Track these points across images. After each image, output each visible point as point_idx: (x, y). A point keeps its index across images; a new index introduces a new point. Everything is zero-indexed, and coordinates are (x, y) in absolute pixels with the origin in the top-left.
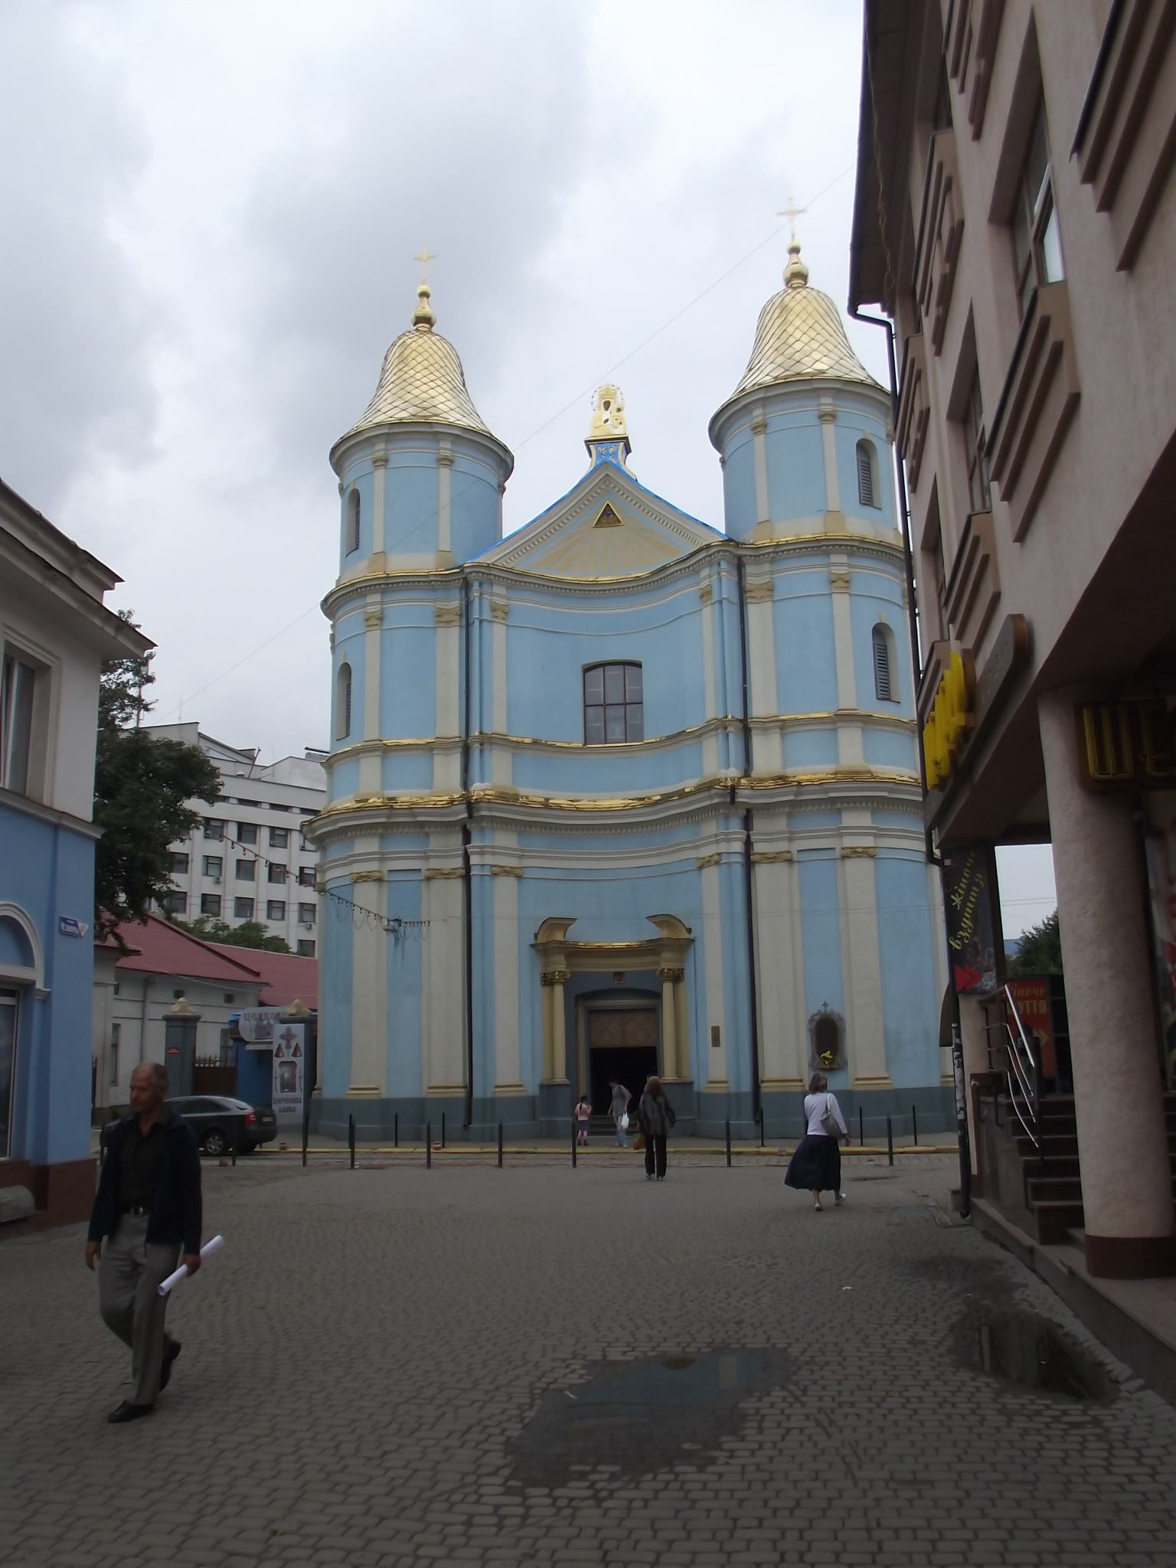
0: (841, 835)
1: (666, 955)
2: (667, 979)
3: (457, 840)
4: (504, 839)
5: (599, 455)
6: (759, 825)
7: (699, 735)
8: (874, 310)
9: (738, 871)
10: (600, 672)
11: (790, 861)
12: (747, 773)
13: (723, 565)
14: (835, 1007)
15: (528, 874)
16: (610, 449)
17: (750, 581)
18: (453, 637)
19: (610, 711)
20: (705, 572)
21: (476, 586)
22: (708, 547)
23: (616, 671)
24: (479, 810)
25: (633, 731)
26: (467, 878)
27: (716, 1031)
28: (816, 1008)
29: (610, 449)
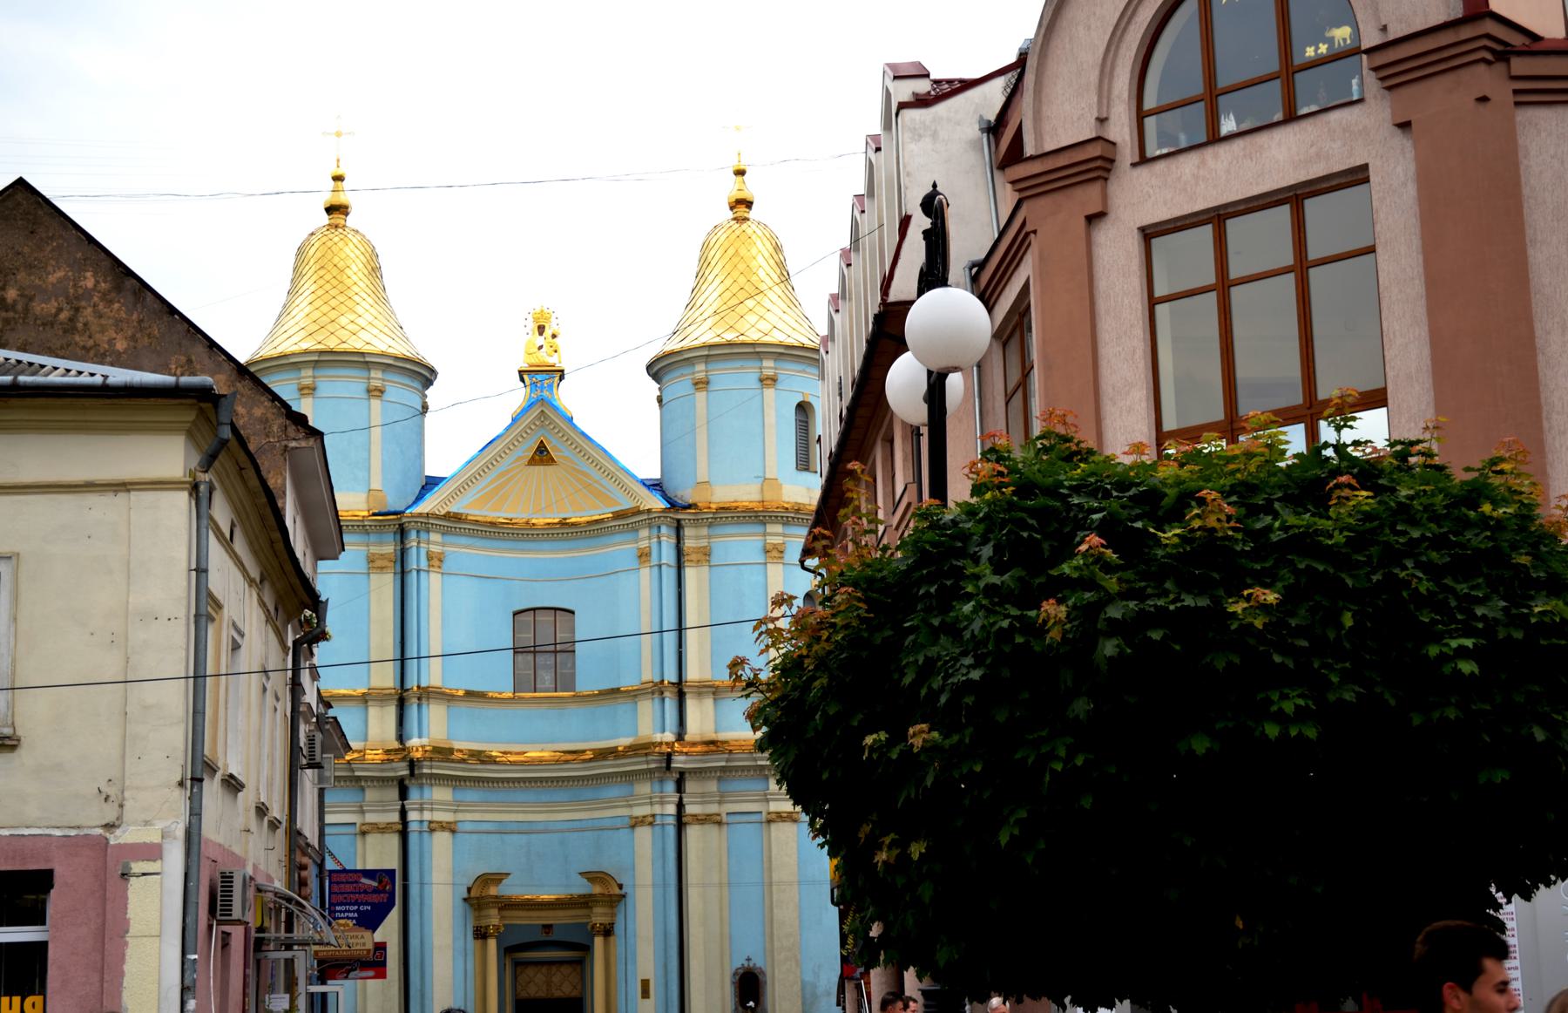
0: (768, 801)
1: (598, 910)
2: (598, 933)
3: (394, 793)
4: (441, 794)
5: (534, 384)
6: (690, 786)
7: (634, 695)
8: (812, 562)
9: (671, 831)
10: (529, 617)
11: (720, 823)
12: (680, 737)
13: (664, 530)
14: (758, 962)
15: (460, 827)
16: (541, 377)
17: (689, 543)
18: (386, 584)
19: (541, 659)
20: (644, 533)
21: (413, 535)
22: (649, 511)
23: (547, 618)
24: (421, 767)
25: (565, 680)
26: (404, 834)
27: (645, 984)
28: (739, 962)
29: (541, 377)
